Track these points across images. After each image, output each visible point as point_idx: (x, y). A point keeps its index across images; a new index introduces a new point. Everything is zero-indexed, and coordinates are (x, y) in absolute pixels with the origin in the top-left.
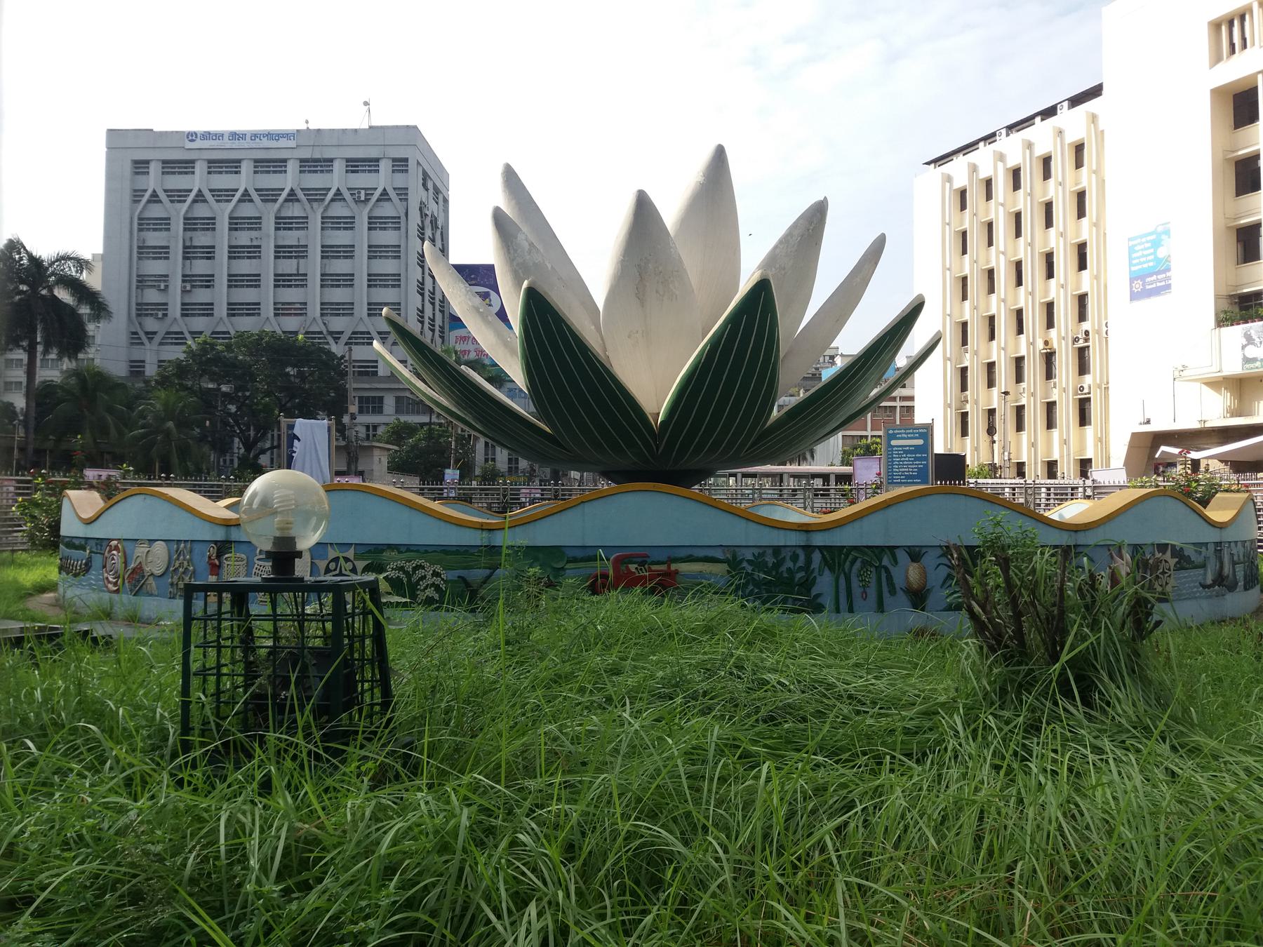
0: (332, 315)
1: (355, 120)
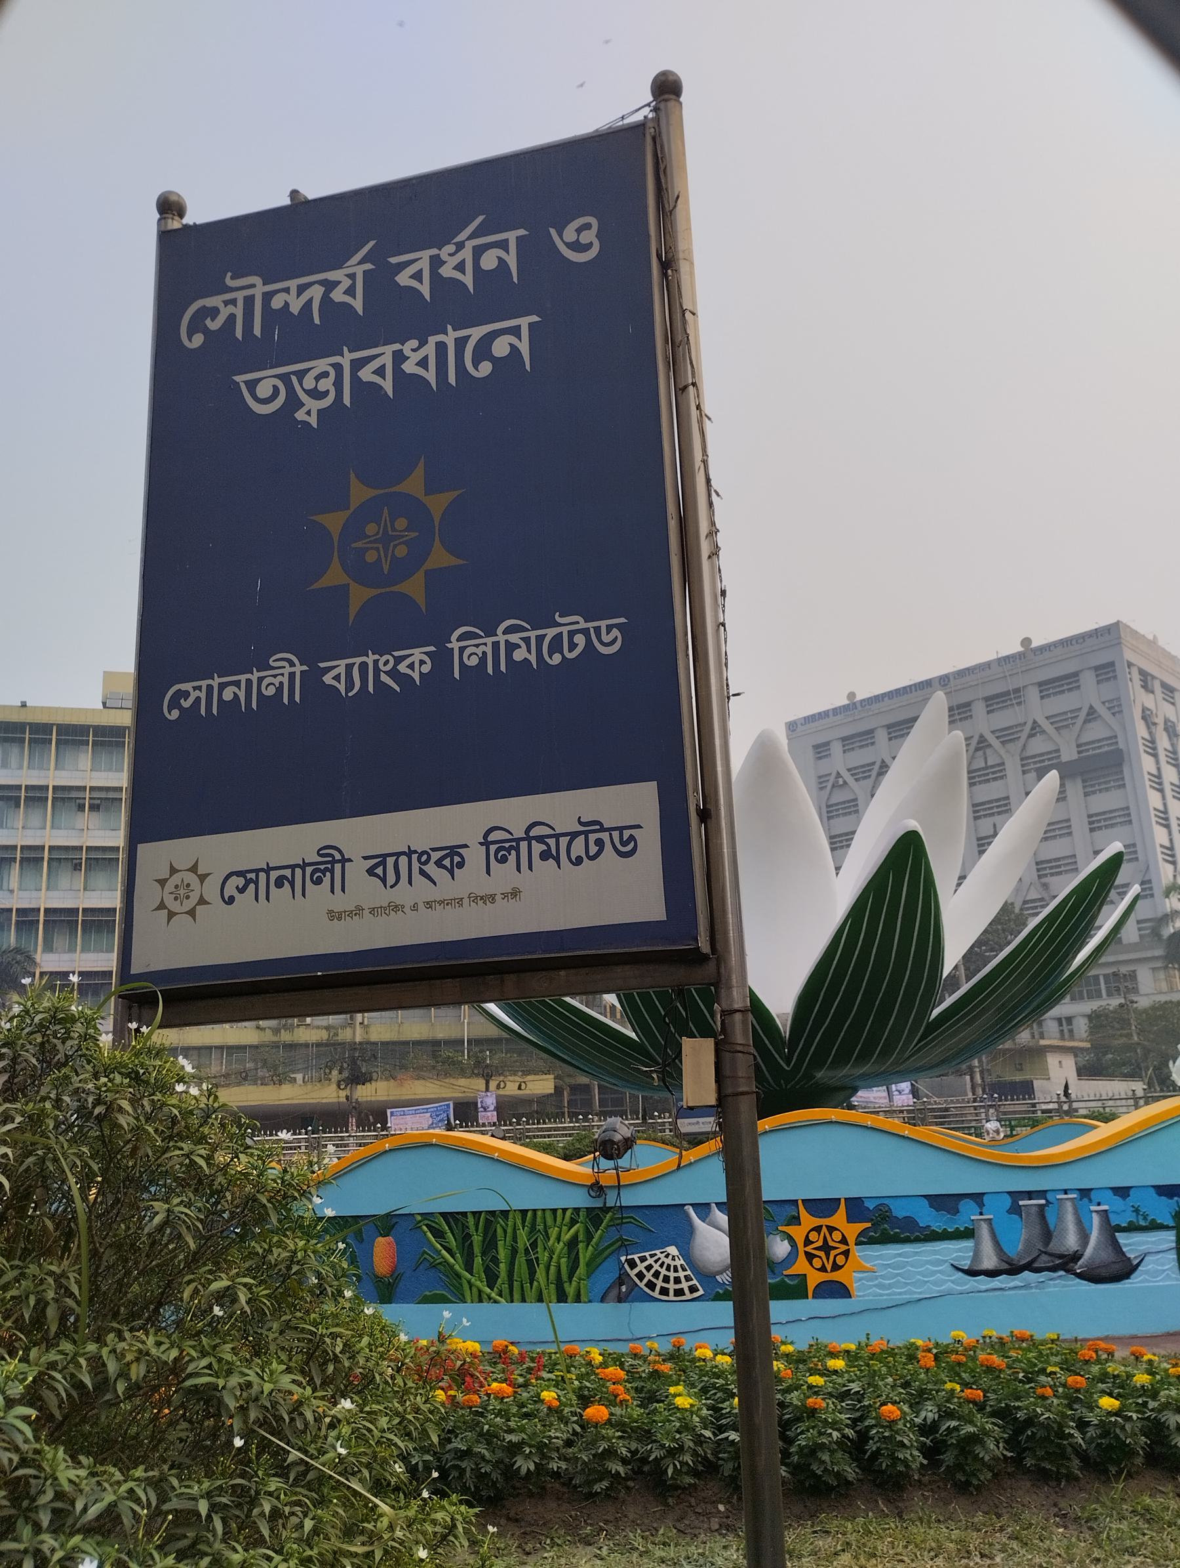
0: (1052, 874)
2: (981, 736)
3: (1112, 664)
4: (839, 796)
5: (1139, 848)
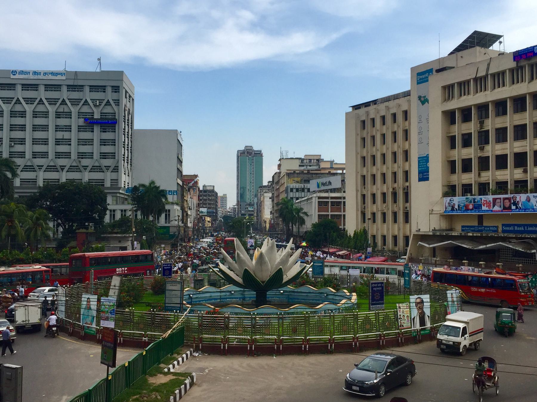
2: (64, 99)
3: (119, 87)
5: (116, 155)
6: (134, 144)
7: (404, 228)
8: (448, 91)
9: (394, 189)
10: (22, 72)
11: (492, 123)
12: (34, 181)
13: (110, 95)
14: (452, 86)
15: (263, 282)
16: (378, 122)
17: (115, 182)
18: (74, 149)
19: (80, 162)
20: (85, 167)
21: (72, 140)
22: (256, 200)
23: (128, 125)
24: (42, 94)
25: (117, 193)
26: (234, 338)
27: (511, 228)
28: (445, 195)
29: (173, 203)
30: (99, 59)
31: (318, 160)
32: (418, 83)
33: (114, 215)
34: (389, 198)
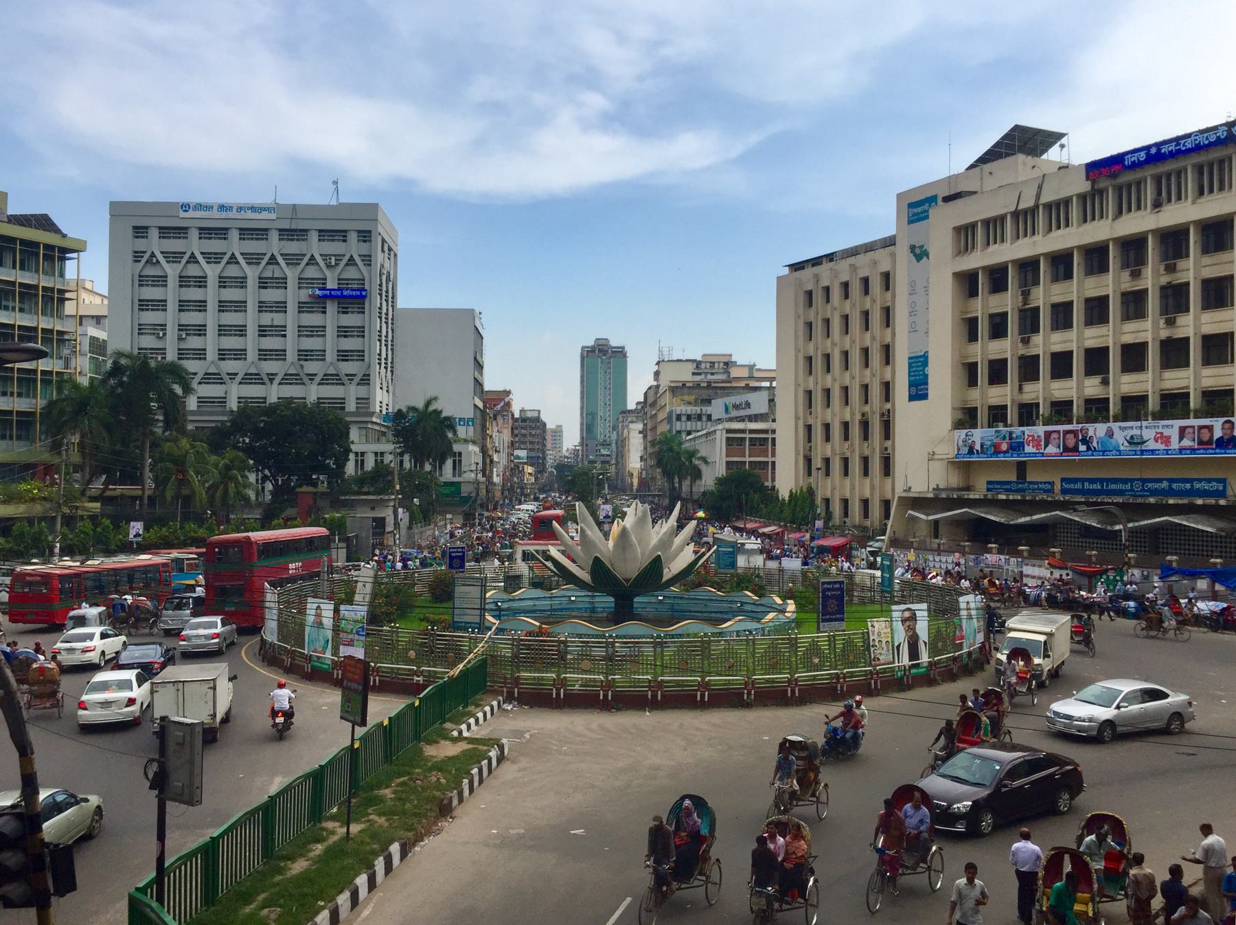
1: (323, 198)
3: (370, 232)
4: (150, 271)
5: (366, 354)
6: (397, 333)
7: (882, 487)
8: (965, 235)
9: (863, 415)
10: (199, 207)
11: (1045, 295)
12: (222, 401)
13: (354, 247)
14: (973, 226)
15: (627, 580)
16: (836, 293)
17: (364, 402)
18: (291, 344)
19: (302, 366)
20: (312, 377)
21: (288, 329)
22: (614, 436)
23: (387, 301)
24: (235, 245)
25: (366, 422)
26: (576, 679)
27: (1078, 486)
28: (958, 425)
29: (466, 441)
30: (335, 183)
31: (726, 364)
32: (910, 222)
33: (362, 461)
34: (855, 431)
